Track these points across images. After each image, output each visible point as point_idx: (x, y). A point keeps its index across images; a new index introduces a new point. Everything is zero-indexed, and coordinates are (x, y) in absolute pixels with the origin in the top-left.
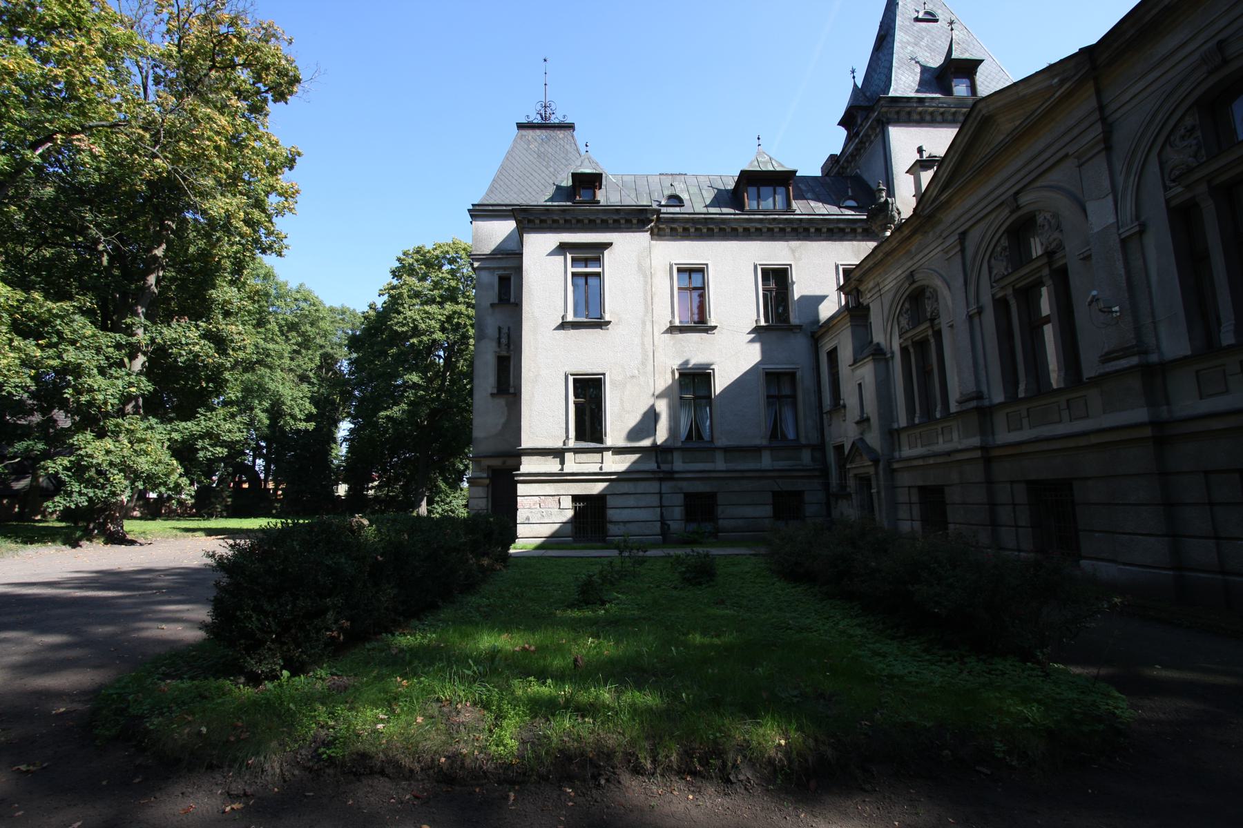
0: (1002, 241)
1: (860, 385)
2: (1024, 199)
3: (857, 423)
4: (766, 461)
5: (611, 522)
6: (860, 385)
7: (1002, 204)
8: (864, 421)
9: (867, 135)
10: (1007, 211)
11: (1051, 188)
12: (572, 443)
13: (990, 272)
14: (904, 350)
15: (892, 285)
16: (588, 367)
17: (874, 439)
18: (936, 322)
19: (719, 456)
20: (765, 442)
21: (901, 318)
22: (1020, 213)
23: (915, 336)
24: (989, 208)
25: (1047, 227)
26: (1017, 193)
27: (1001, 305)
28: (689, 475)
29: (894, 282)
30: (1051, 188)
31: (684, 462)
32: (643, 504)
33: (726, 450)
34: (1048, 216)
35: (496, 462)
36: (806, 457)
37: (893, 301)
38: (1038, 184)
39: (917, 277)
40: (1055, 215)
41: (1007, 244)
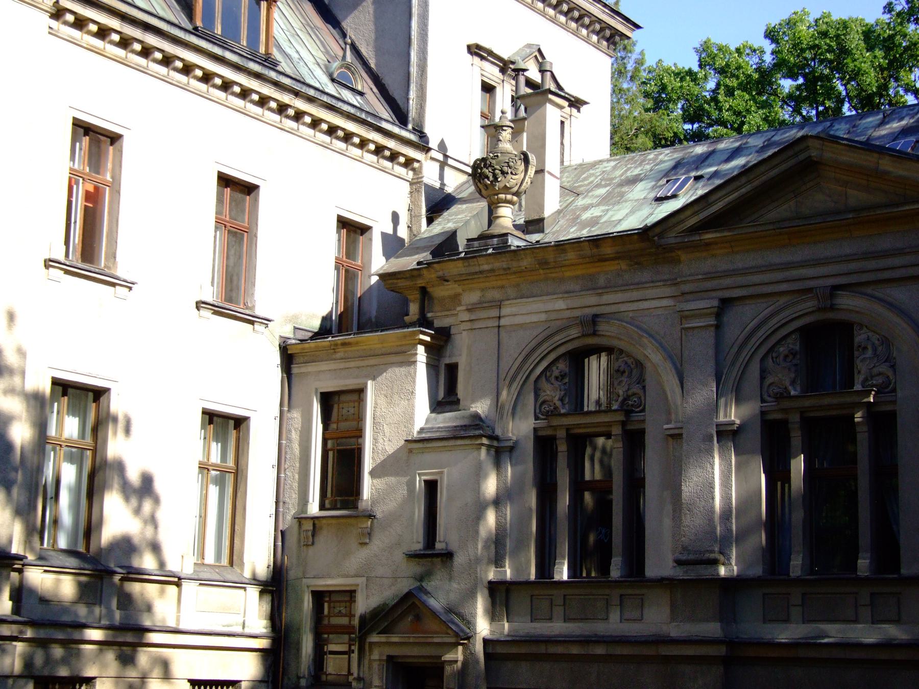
0: (789, 341)
2: (848, 302)
7: (809, 290)
10: (810, 304)
11: (891, 306)
13: (762, 378)
15: (534, 318)
18: (636, 417)
21: (544, 384)
22: (831, 315)
23: (579, 426)
24: (784, 287)
25: (869, 353)
26: (836, 288)
29: (543, 317)
30: (891, 306)
34: (875, 338)
37: (534, 350)
38: (869, 290)
39: (603, 327)
40: (886, 342)
41: (797, 348)
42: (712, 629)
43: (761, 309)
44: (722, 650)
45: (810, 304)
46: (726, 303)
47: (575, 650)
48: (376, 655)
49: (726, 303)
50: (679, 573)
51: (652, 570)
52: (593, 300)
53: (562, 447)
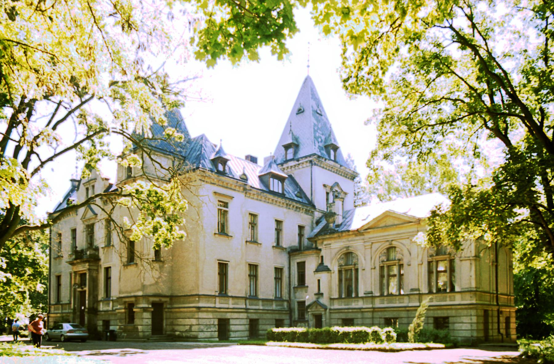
1: (319, 281)
3: (315, 294)
4: (274, 307)
5: (232, 331)
6: (319, 281)
8: (319, 294)
9: (303, 163)
11: (402, 243)
12: (217, 294)
14: (340, 272)
16: (224, 257)
17: (324, 300)
19: (260, 303)
20: (273, 298)
27: (382, 268)
28: (252, 311)
30: (402, 243)
31: (263, 305)
32: (241, 323)
33: (263, 300)
35: (156, 299)
36: (285, 304)
39: (350, 248)
40: (401, 250)
42: (370, 306)
43: (379, 244)
44: (372, 310)
45: (388, 243)
46: (372, 243)
47: (346, 311)
48: (310, 313)
49: (372, 243)
50: (365, 295)
51: (360, 295)
52: (348, 243)
53: (343, 272)
